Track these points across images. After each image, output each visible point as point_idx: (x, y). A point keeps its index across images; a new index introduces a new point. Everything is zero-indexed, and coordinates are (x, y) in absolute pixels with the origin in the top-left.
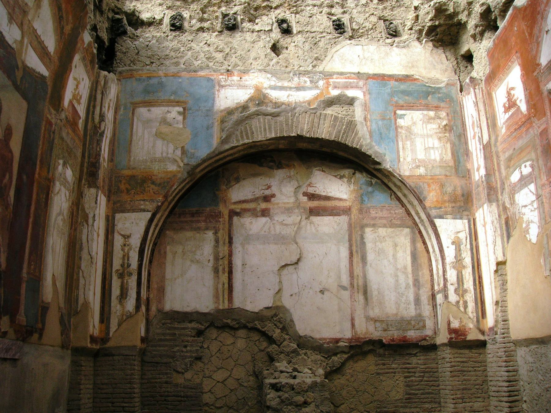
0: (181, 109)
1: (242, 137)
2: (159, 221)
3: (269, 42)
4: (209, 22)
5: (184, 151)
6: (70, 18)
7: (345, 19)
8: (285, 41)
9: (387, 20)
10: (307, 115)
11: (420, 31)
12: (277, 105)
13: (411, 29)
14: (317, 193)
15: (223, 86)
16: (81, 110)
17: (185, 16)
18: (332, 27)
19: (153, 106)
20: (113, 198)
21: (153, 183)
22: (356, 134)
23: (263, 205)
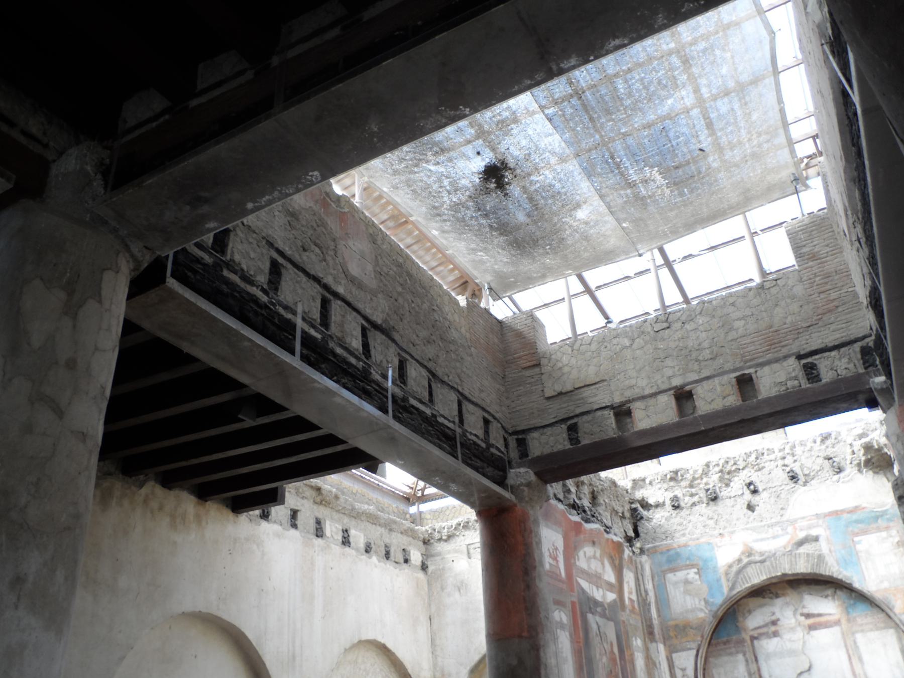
0: (696, 570)
1: (743, 583)
2: (702, 653)
3: (744, 504)
4: (697, 496)
5: (706, 602)
6: (617, 556)
7: (797, 469)
8: (756, 499)
9: (831, 458)
10: (786, 557)
11: (859, 465)
12: (761, 554)
13: (851, 463)
14: (811, 612)
15: (720, 547)
16: (634, 597)
17: (680, 495)
18: (788, 479)
19: (676, 571)
20: (668, 643)
21: (691, 628)
22: (827, 564)
23: (773, 628)
